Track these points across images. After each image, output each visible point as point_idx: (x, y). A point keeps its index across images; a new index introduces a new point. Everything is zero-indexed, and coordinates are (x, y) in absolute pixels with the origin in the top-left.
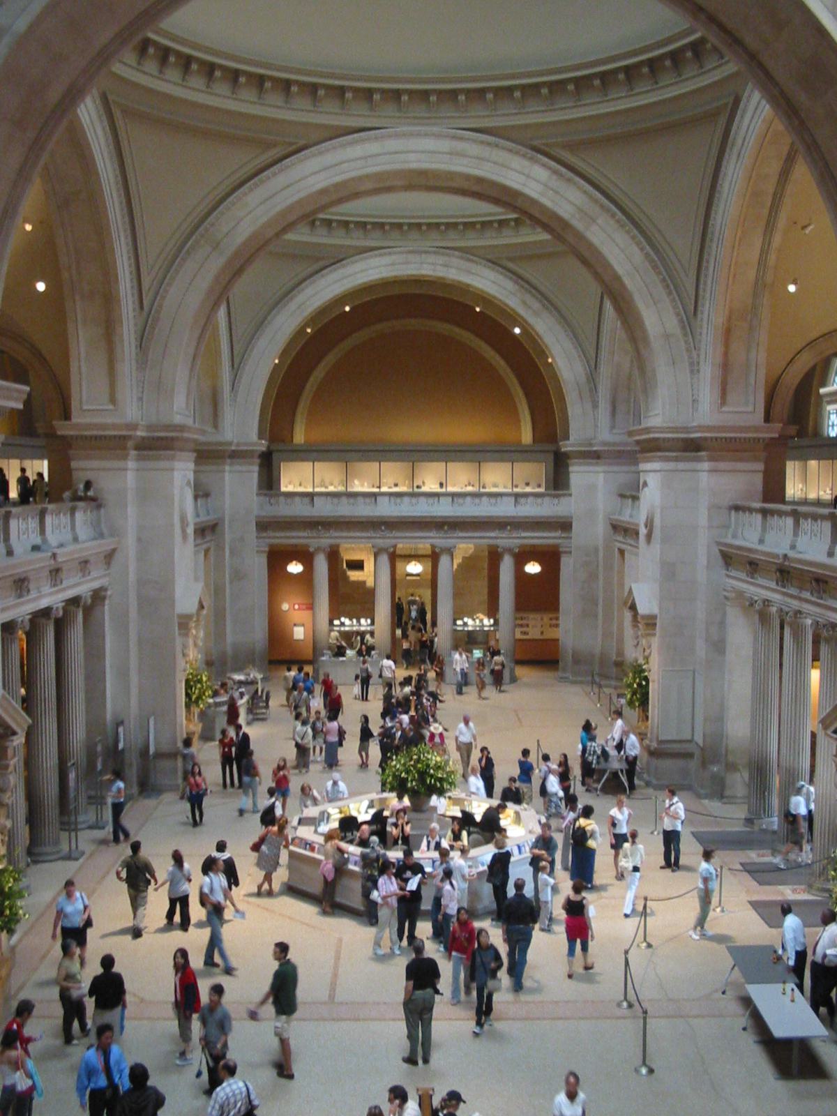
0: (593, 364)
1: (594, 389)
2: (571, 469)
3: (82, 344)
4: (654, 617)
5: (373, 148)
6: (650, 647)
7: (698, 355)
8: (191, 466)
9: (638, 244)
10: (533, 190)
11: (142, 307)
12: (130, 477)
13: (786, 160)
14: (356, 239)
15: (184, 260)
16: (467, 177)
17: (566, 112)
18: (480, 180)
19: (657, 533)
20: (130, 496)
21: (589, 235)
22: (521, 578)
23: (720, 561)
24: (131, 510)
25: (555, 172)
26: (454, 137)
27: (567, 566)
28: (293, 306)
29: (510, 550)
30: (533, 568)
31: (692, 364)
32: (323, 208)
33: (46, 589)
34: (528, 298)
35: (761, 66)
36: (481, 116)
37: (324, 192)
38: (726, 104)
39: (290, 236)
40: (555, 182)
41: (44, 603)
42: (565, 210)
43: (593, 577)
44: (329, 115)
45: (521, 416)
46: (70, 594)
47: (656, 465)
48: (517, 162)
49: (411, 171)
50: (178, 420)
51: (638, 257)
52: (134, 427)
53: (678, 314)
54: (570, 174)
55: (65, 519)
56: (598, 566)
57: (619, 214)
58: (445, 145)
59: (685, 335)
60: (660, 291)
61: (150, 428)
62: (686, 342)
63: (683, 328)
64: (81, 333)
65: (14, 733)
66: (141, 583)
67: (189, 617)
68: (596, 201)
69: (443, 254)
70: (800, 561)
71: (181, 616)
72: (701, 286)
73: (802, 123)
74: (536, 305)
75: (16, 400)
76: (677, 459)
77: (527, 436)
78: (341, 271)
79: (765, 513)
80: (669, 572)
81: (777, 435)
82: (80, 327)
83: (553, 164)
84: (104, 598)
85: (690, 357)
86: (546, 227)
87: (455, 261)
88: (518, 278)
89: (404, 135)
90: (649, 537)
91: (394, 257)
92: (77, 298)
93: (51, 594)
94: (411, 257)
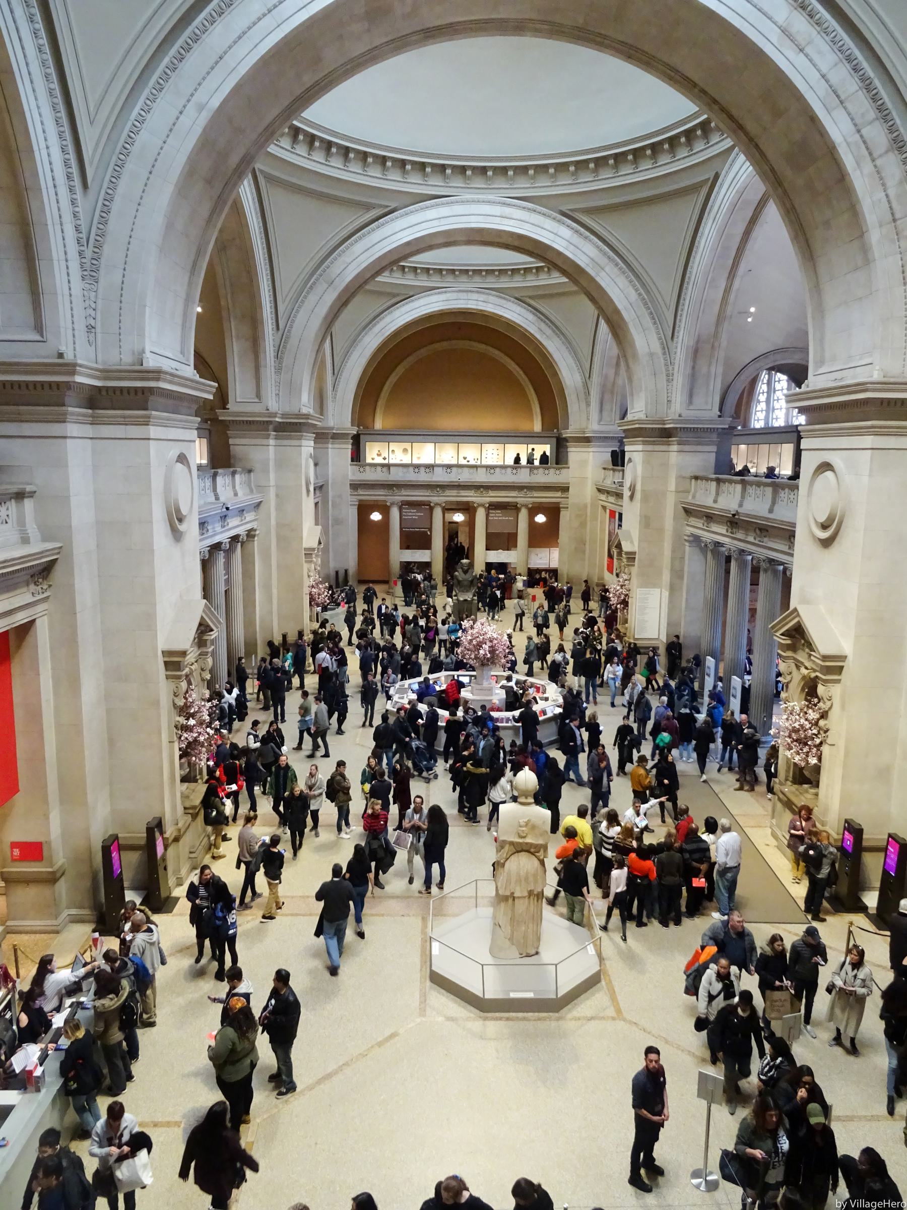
1: (588, 393)
2: (569, 449)
4: (635, 553)
5: (444, 211)
7: (673, 369)
8: (312, 443)
9: (634, 286)
10: (559, 245)
11: (278, 329)
12: (271, 449)
13: (750, 222)
15: (308, 293)
16: (512, 234)
17: (587, 183)
18: (521, 237)
19: (638, 495)
20: (272, 463)
21: (598, 279)
22: (532, 524)
24: (272, 476)
25: (577, 231)
26: (504, 204)
28: (377, 329)
29: (526, 506)
30: (540, 519)
31: (668, 375)
32: (405, 257)
33: (218, 528)
34: (543, 326)
35: (757, 146)
36: (523, 187)
37: (408, 244)
38: (709, 179)
39: (379, 279)
40: (576, 239)
41: (216, 539)
42: (582, 261)
43: (583, 525)
44: (414, 184)
46: (233, 533)
47: (640, 447)
48: (549, 224)
49: (472, 229)
50: (304, 410)
51: (633, 295)
52: (275, 415)
53: (660, 339)
54: (588, 234)
55: (228, 479)
57: (622, 264)
58: (497, 210)
59: (664, 354)
60: (647, 321)
61: (284, 416)
63: (664, 348)
64: (235, 343)
65: (212, 630)
66: (279, 525)
67: (313, 549)
68: (605, 254)
69: (483, 293)
70: (748, 515)
71: (305, 549)
72: (678, 318)
73: (785, 192)
74: (549, 332)
75: (209, 392)
76: (653, 443)
77: (537, 427)
79: (718, 481)
80: (646, 522)
81: (727, 426)
82: (234, 339)
83: (574, 225)
84: (254, 536)
85: (667, 370)
86: (564, 272)
87: (492, 299)
89: (468, 202)
90: (632, 497)
93: (221, 532)
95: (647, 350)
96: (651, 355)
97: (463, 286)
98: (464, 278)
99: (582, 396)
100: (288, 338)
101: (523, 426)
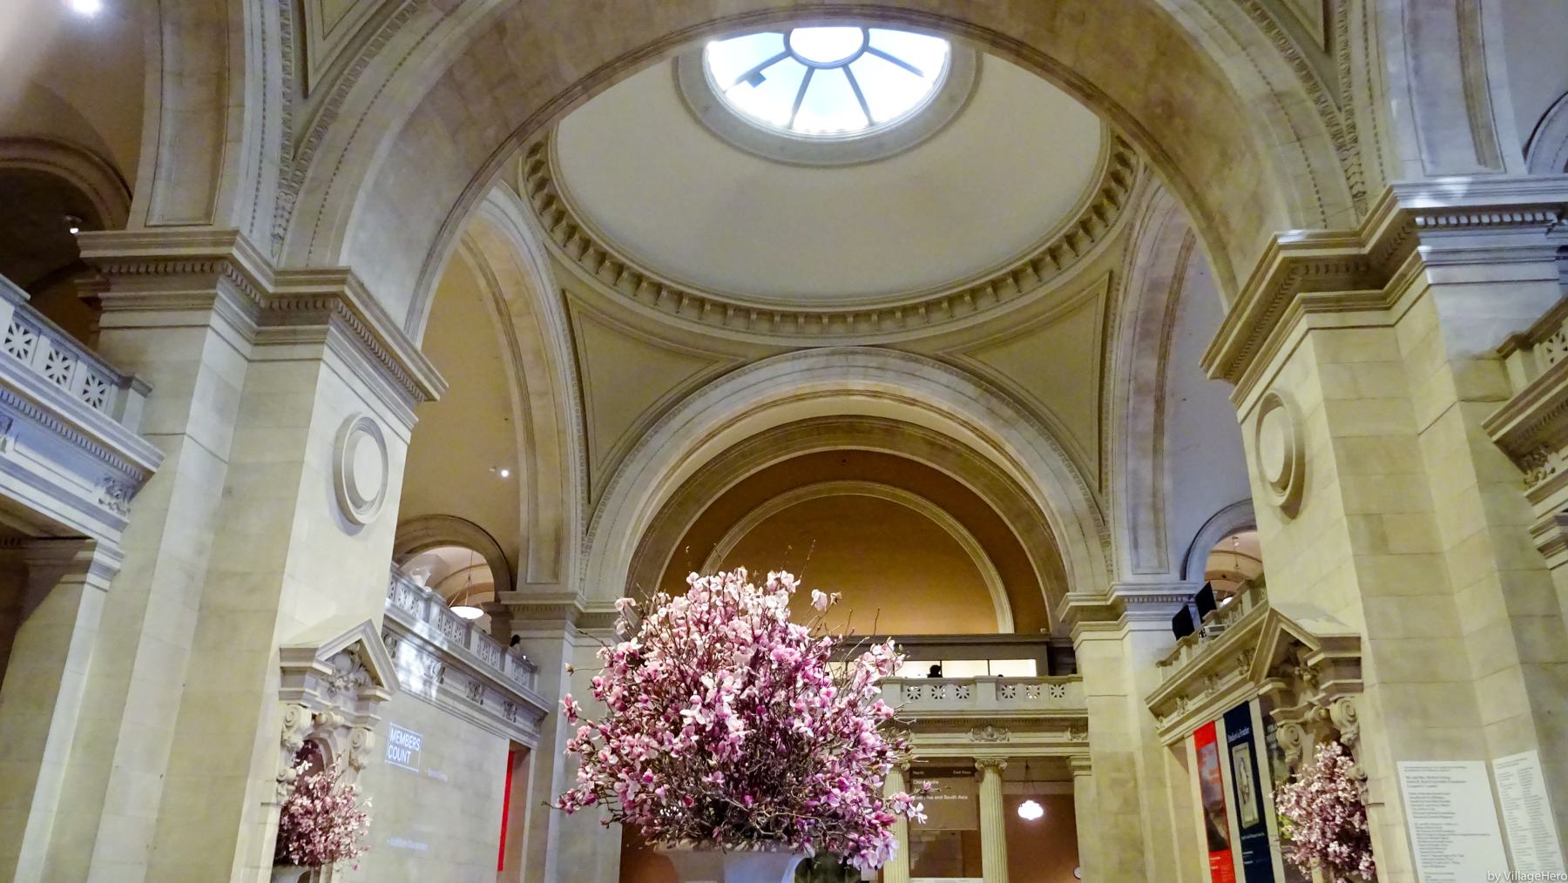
0: (1096, 485)
1: (1102, 522)
3: (168, 118)
6: (1353, 719)
11: (305, 95)
14: (762, 338)
22: (1014, 829)
23: (1507, 464)
27: (1086, 792)
29: (994, 765)
30: (1031, 811)
43: (1131, 805)
45: (998, 612)
56: (1136, 786)
62: (1317, 101)
69: (877, 355)
71: (283, 652)
74: (1008, 412)
77: (1005, 626)
78: (741, 379)
88: (976, 377)
91: (810, 362)
92: (168, 29)
94: (835, 360)
95: (1262, 89)
96: (1277, 97)
97: (839, 344)
98: (838, 328)
99: (1089, 524)
100: (331, 115)
101: (980, 627)
